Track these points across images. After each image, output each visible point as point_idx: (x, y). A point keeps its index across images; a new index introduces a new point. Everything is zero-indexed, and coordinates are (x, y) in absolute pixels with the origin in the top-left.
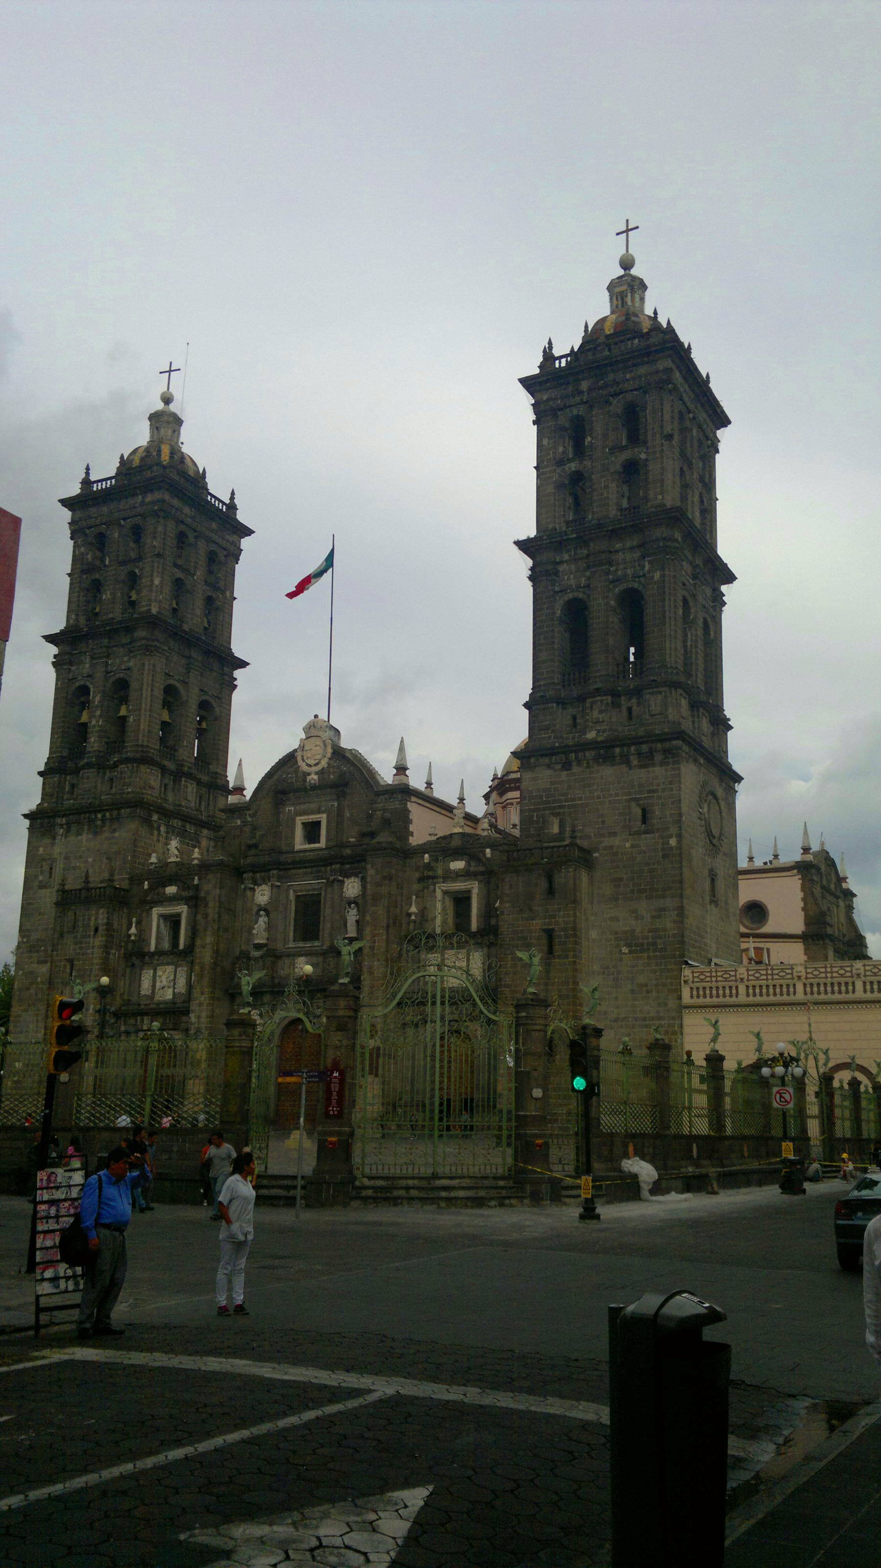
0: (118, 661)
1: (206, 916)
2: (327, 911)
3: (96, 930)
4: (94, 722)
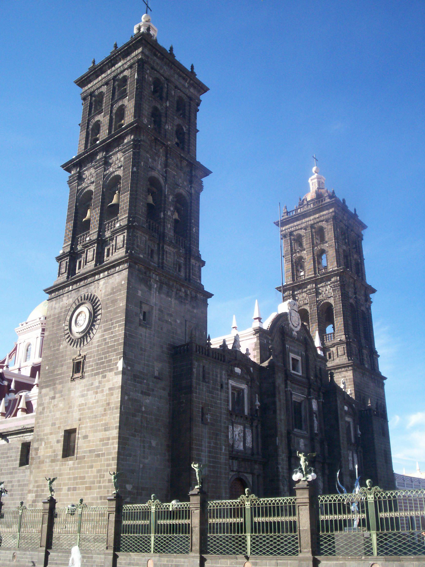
3: (222, 386)
4: (169, 213)
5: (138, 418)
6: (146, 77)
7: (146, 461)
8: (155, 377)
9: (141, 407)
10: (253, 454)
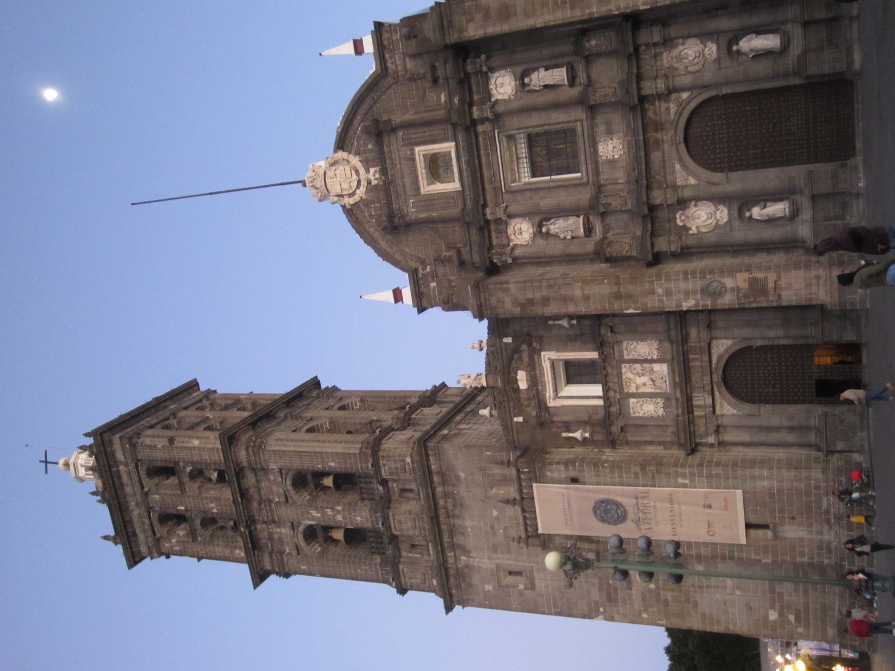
0: (275, 489)
1: (546, 301)
2: (535, 121)
3: (574, 480)
4: (339, 518)
5: (669, 596)
6: (177, 548)
9: (651, 591)
10: (672, 343)
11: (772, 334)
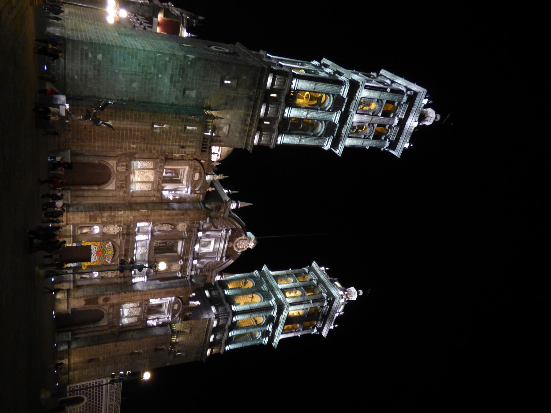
5: (152, 70)
7: (120, 77)
8: (184, 90)
9: (161, 73)
11: (90, 193)
